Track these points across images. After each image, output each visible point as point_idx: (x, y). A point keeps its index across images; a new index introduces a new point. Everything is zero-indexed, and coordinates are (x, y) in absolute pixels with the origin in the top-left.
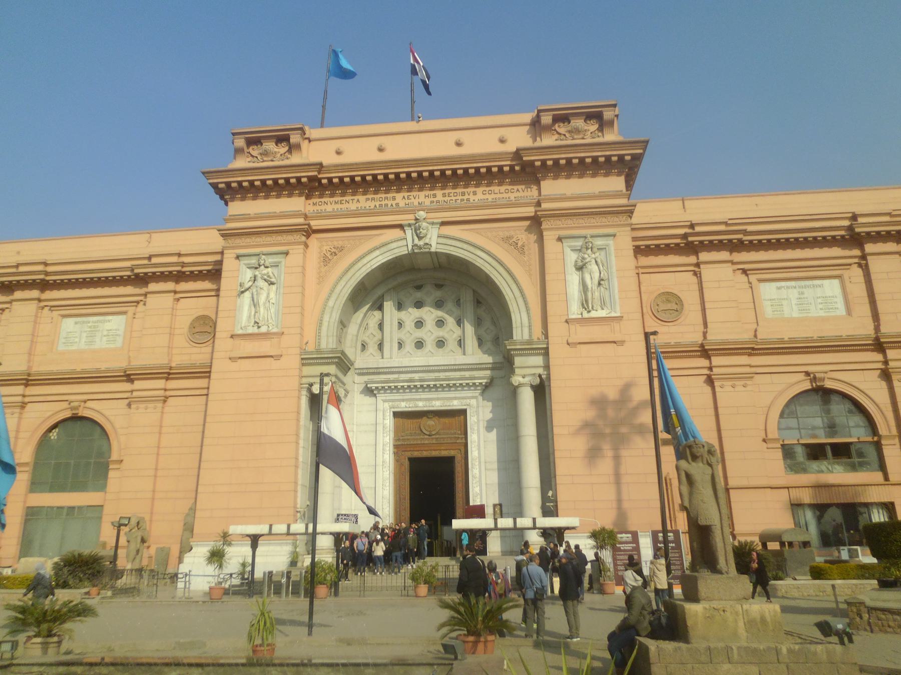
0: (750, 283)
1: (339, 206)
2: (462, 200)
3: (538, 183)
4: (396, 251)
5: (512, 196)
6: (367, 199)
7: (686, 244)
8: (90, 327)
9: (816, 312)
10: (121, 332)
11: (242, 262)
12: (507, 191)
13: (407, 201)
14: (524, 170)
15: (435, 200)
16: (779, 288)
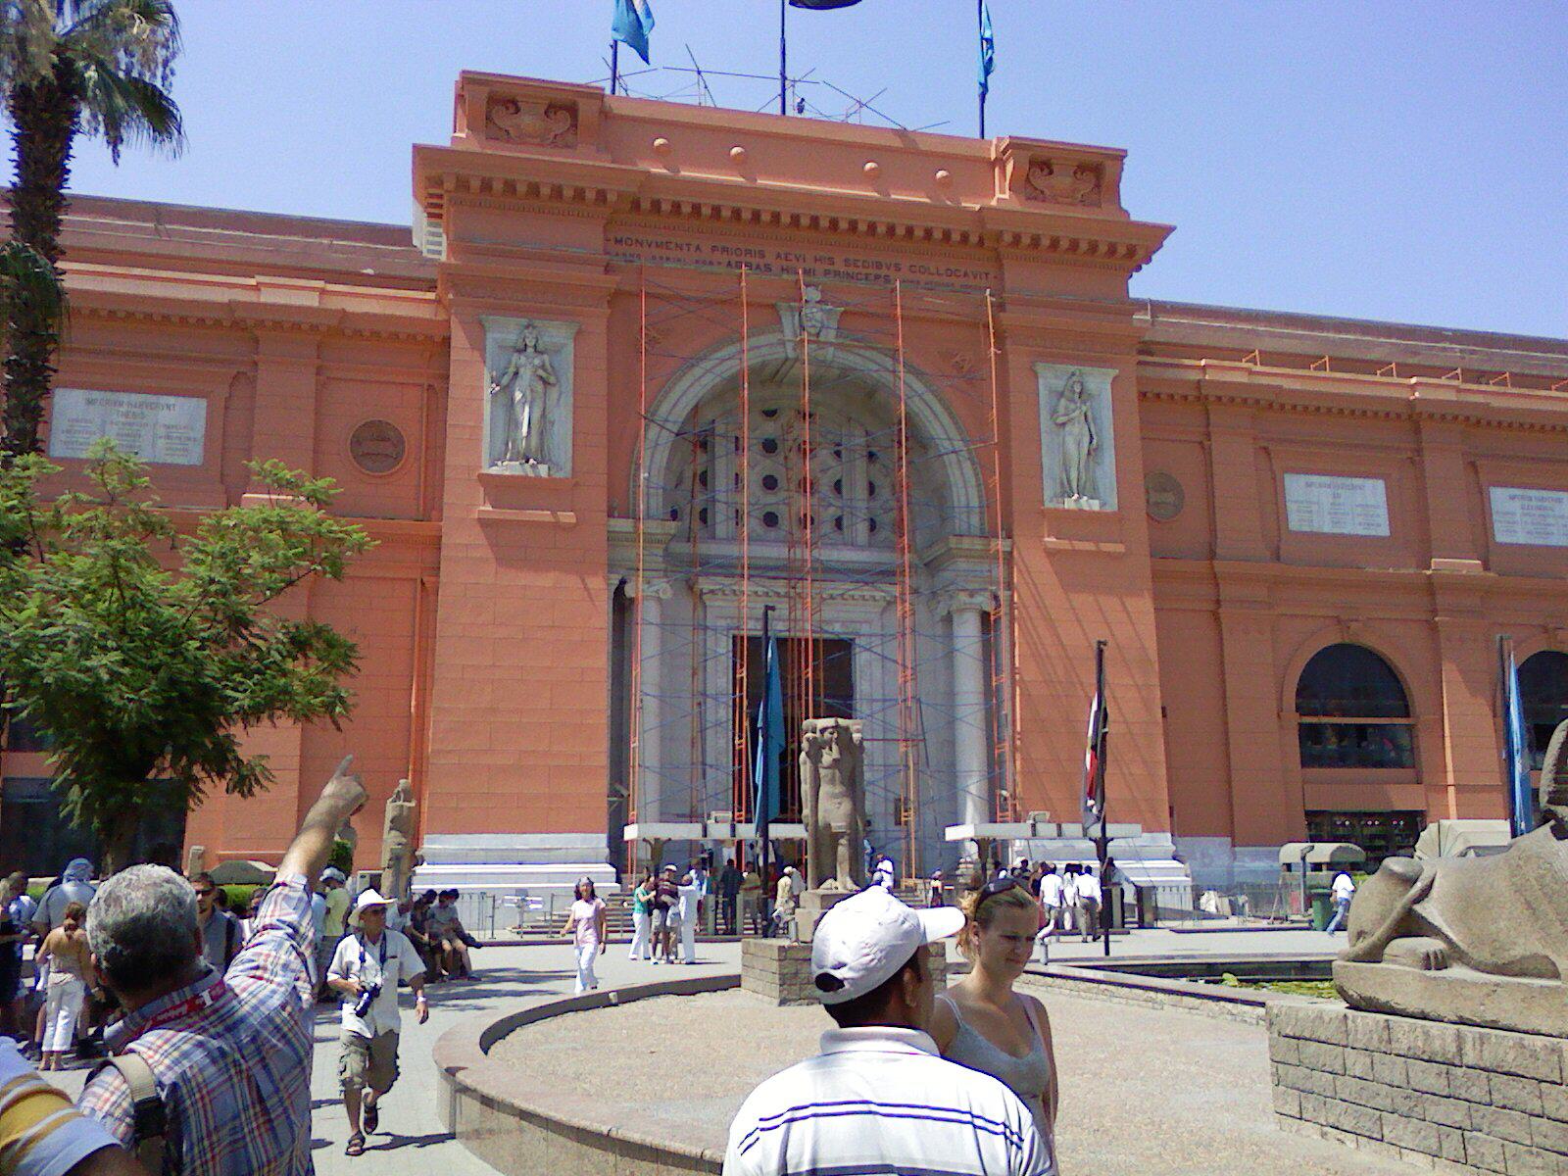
0: (1273, 472)
1: (665, 253)
2: (877, 277)
3: (1001, 267)
4: (764, 351)
5: (958, 282)
6: (714, 249)
7: (1198, 398)
8: (126, 415)
9: (1353, 527)
10: (199, 430)
11: (490, 336)
12: (950, 273)
13: (785, 264)
14: (986, 244)
15: (831, 267)
16: (1309, 485)
